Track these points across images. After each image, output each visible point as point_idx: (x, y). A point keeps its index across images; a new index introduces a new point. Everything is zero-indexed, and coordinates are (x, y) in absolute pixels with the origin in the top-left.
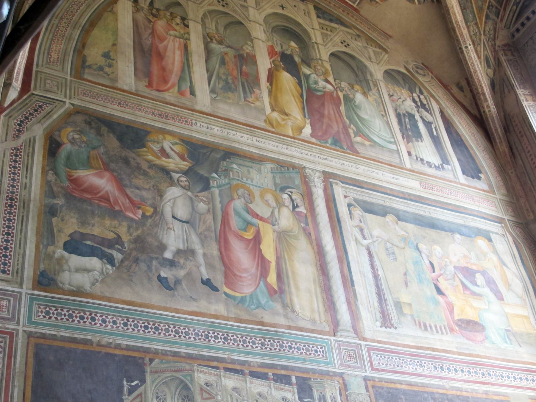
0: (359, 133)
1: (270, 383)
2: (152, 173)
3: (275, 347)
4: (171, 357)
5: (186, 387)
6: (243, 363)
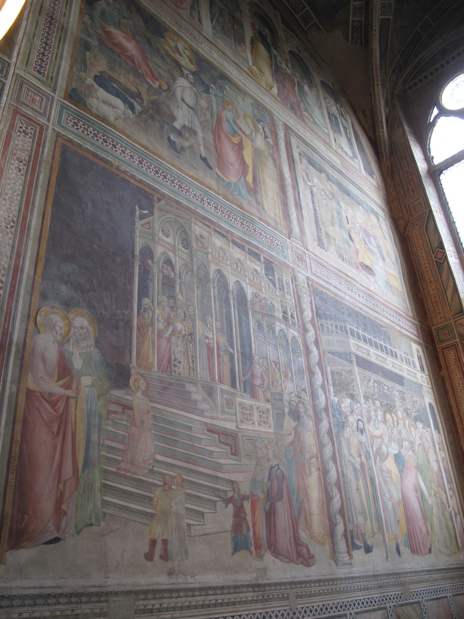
0: (306, 110)
2: (168, 60)
5: (185, 232)
6: (229, 232)
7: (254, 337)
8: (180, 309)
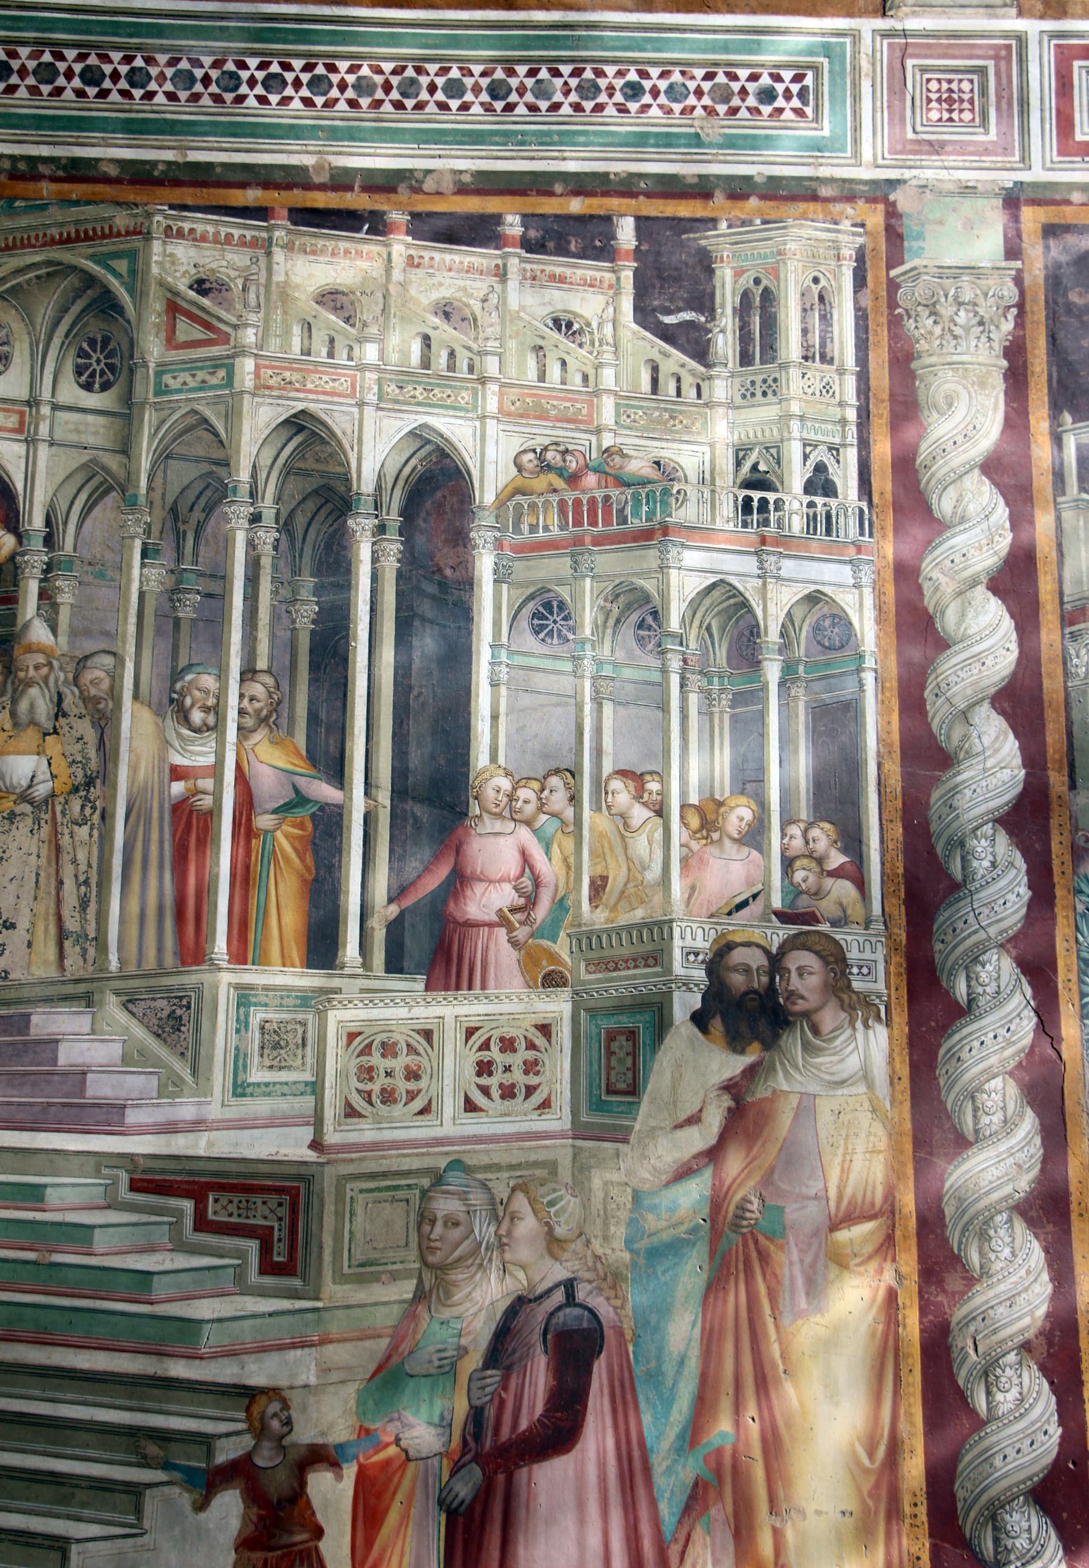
1: (505, 256)
3: (558, 97)
4: (54, 187)
7: (494, 684)
8: (34, 691)
